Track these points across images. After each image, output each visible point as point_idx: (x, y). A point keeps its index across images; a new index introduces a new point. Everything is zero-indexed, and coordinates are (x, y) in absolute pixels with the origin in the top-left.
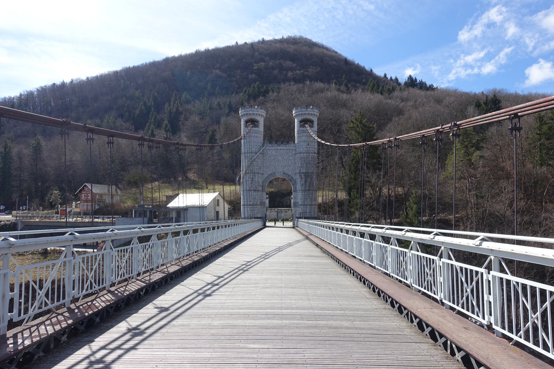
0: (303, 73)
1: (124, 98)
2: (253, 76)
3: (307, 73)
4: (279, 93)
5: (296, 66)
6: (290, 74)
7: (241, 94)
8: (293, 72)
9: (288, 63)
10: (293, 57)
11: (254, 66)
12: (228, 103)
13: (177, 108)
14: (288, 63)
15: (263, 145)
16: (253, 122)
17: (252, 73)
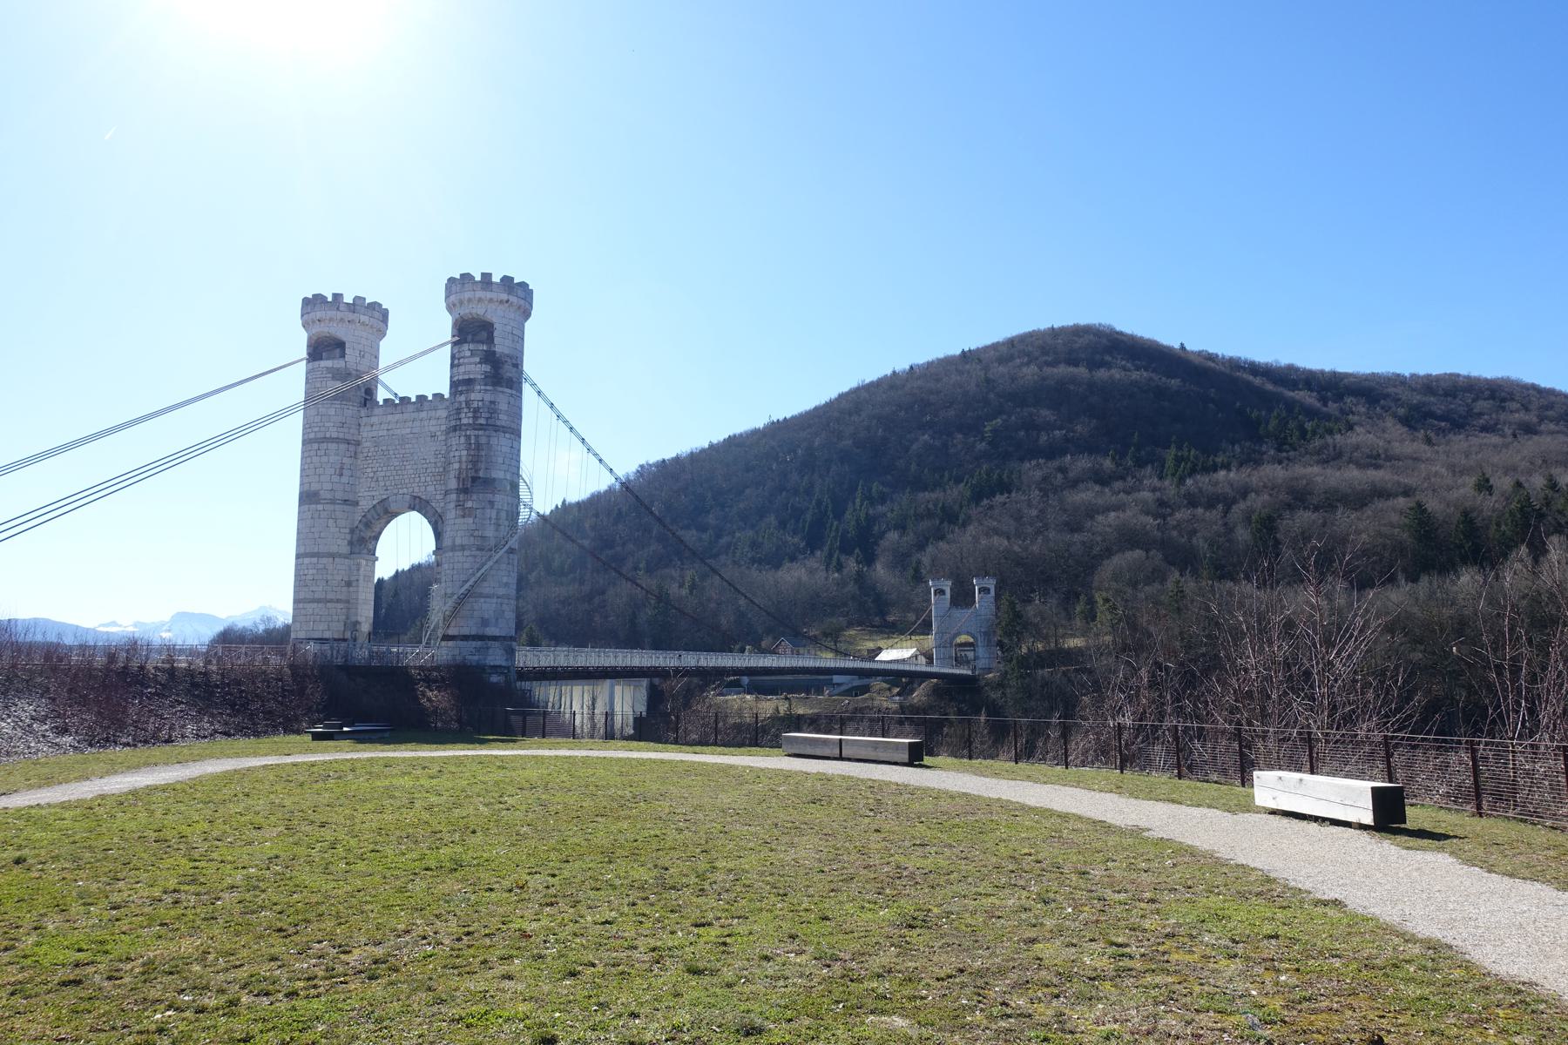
0: (1065, 435)
1: (784, 493)
2: (981, 446)
3: (1072, 434)
4: (1010, 492)
5: (1055, 420)
6: (1044, 438)
7: (962, 484)
8: (1049, 435)
9: (1046, 414)
10: (1058, 395)
11: (985, 427)
12: (940, 505)
13: (866, 514)
14: (1046, 414)
15: (950, 609)
16: (942, 592)
17: (983, 439)
